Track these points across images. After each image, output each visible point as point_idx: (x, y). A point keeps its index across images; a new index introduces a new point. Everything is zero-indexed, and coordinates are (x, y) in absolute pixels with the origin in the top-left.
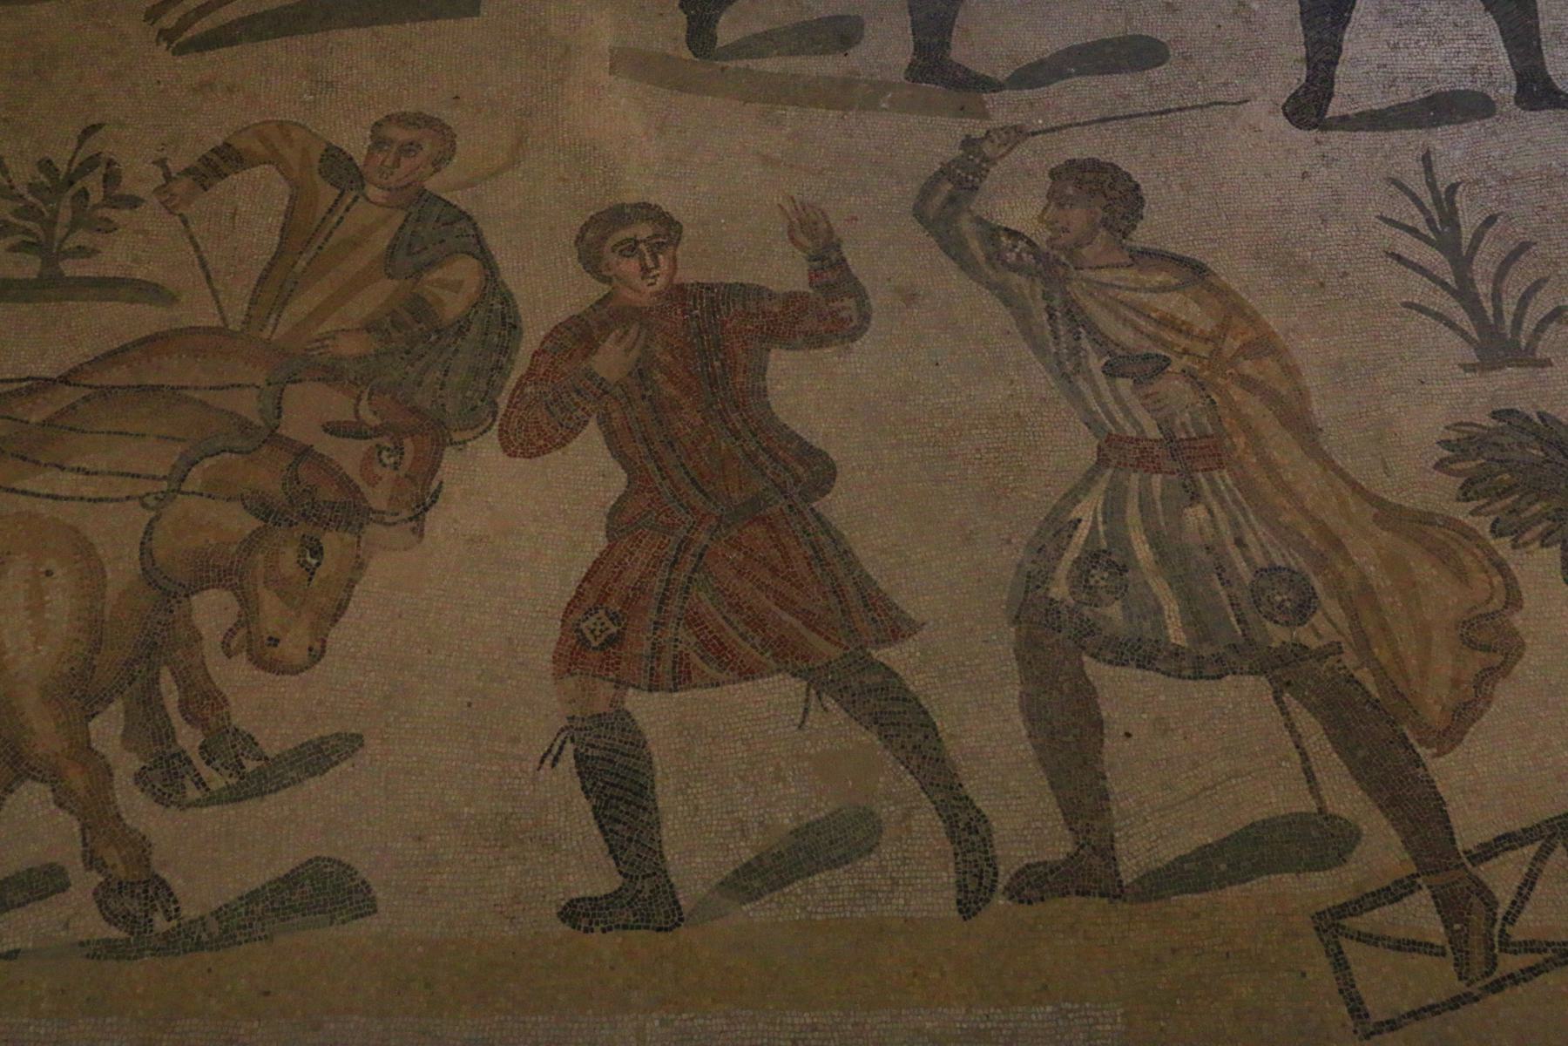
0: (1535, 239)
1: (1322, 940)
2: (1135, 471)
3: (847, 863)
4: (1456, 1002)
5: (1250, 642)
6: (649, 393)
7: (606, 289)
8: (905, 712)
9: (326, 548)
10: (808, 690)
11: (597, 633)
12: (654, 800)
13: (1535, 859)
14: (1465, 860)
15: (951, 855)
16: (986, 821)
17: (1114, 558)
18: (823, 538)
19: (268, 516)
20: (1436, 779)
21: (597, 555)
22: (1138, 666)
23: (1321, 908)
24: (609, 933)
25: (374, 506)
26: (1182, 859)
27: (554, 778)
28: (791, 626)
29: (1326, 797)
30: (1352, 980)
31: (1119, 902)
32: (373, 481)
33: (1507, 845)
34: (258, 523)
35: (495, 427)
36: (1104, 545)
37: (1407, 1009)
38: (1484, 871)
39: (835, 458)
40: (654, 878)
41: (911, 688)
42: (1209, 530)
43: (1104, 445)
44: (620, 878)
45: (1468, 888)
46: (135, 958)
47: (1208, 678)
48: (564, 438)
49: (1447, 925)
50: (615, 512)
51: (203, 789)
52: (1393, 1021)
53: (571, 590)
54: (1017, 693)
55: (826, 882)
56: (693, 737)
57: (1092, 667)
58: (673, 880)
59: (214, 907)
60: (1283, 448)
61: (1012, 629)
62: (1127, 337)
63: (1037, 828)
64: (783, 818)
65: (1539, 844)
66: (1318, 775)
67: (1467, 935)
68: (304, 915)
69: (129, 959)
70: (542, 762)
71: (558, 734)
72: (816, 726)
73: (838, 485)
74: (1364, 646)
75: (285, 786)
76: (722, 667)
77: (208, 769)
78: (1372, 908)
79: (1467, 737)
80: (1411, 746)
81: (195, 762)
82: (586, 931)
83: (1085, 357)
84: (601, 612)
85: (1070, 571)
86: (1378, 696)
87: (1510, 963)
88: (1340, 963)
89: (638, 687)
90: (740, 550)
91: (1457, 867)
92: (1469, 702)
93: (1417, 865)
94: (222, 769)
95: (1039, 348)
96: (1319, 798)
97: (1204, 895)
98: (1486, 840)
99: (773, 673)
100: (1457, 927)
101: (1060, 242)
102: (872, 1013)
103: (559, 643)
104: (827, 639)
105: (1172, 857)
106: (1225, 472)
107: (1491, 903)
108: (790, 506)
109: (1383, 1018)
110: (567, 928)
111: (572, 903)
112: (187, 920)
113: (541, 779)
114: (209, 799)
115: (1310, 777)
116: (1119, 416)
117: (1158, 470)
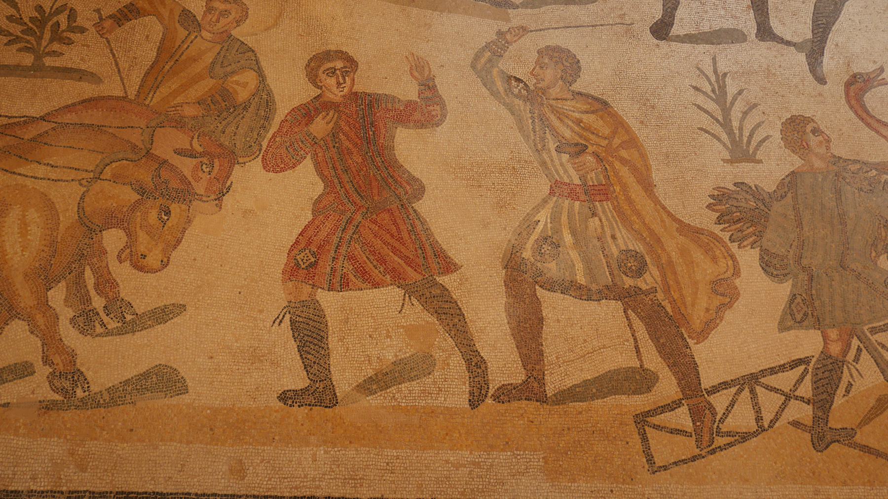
0: (760, 102)
1: (637, 427)
2: (567, 199)
3: (418, 379)
4: (694, 459)
5: (615, 285)
6: (337, 145)
7: (319, 91)
8: (450, 308)
10: (405, 295)
11: (305, 261)
12: (327, 344)
13: (735, 394)
14: (704, 393)
15: (467, 378)
16: (485, 363)
17: (554, 241)
19: (144, 193)
20: (695, 354)
21: (307, 223)
22: (562, 293)
23: (637, 413)
24: (302, 408)
25: (198, 192)
26: (575, 386)
27: (280, 331)
28: (399, 263)
29: (644, 360)
30: (649, 446)
31: (545, 404)
32: (198, 180)
33: (724, 387)
35: (261, 156)
36: (550, 233)
37: (673, 461)
38: (712, 399)
39: (425, 183)
40: (325, 382)
41: (454, 296)
42: (599, 230)
43: (554, 185)
44: (308, 381)
45: (705, 406)
46: (67, 410)
47: (594, 300)
48: (294, 164)
50: (318, 201)
51: (104, 328)
52: (666, 466)
53: (293, 239)
54: (504, 302)
55: (408, 388)
56: (348, 314)
57: (540, 292)
58: (334, 383)
59: (107, 387)
60: (636, 192)
61: (504, 271)
62: (568, 134)
63: (509, 367)
64: (389, 356)
65: (738, 387)
66: (641, 350)
67: (702, 428)
68: (152, 392)
69: (63, 410)
70: (274, 322)
71: (283, 310)
72: (407, 312)
73: (425, 196)
74: (667, 290)
75: (145, 329)
76: (365, 281)
77: (108, 318)
78: (661, 413)
79: (710, 336)
80: (685, 338)
81: (101, 314)
82: (290, 406)
83: (548, 142)
84: (307, 251)
85: (533, 245)
86: (672, 314)
87: (720, 441)
88: (644, 439)
89: (323, 289)
90: (376, 225)
91: (701, 396)
92: (713, 320)
93: (683, 394)
94: (114, 319)
95: (526, 137)
96: (641, 360)
97: (585, 403)
98: (714, 384)
99: (388, 285)
100: (698, 424)
101: (540, 86)
102: (425, 452)
103: (285, 265)
104: (415, 270)
105: (571, 385)
106: (609, 202)
107: (714, 414)
108: (402, 205)
109: (661, 465)
110: (281, 404)
111: (284, 392)
112: (93, 392)
113: (273, 331)
114: (107, 333)
115: (638, 351)
116: (561, 172)
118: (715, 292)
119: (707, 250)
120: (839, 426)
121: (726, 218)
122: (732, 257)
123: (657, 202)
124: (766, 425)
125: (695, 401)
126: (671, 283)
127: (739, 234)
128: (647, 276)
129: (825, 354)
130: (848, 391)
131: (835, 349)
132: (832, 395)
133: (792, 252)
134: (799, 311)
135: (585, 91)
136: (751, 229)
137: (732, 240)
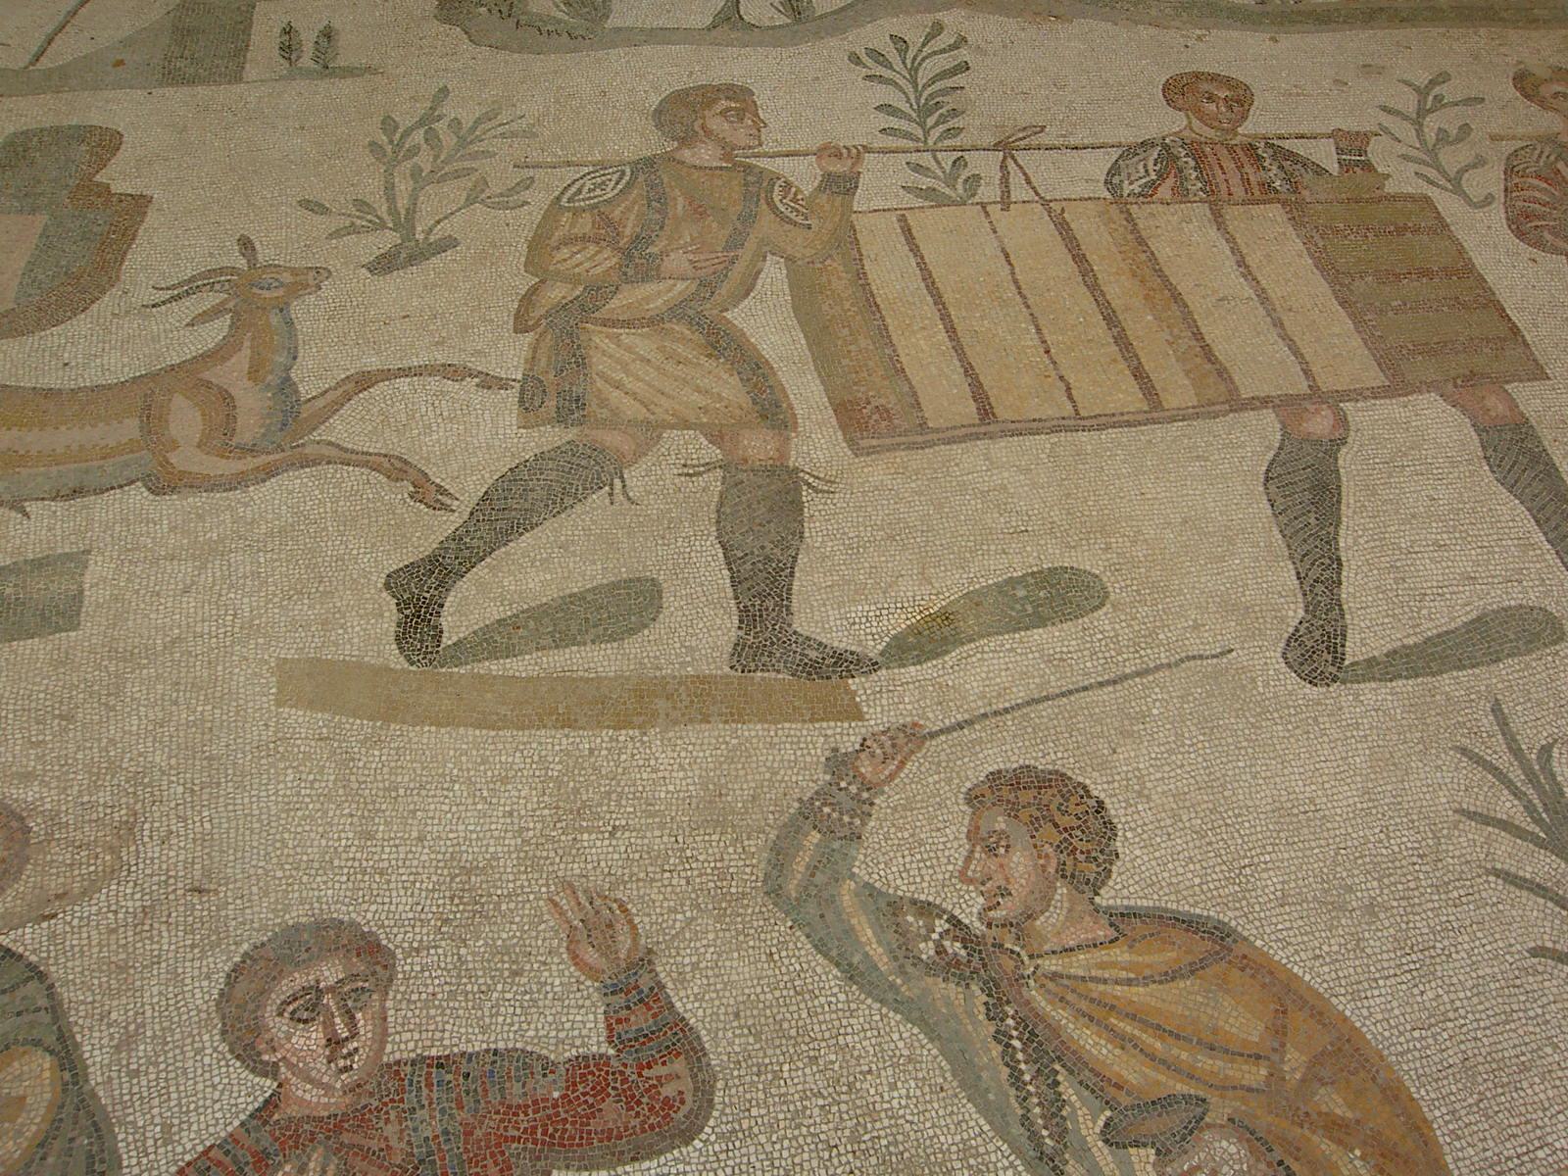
135: (1145, 903)
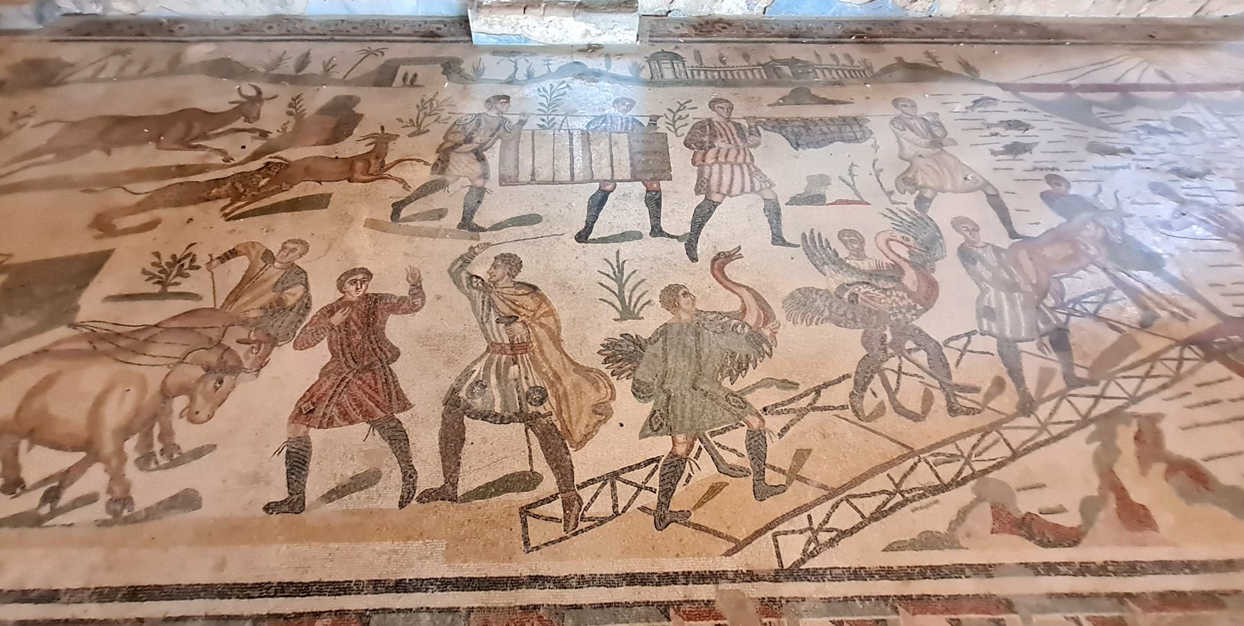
5: (521, 411)
9: (224, 382)
18: (390, 377)
34: (204, 373)
36: (481, 379)
38: (580, 492)
42: (517, 374)
49: (565, 512)
76: (345, 420)
87: (582, 525)
96: (531, 465)
107: (581, 504)
116: (497, 336)
117: (505, 354)
118: (595, 412)
119: (594, 383)
120: (678, 510)
121: (611, 359)
122: (611, 387)
123: (562, 351)
124: (620, 512)
125: (568, 494)
126: (564, 407)
127: (620, 370)
128: (546, 404)
129: (673, 454)
130: (687, 481)
131: (681, 450)
132: (674, 485)
133: (656, 380)
134: (656, 423)
136: (629, 366)
137: (613, 375)
